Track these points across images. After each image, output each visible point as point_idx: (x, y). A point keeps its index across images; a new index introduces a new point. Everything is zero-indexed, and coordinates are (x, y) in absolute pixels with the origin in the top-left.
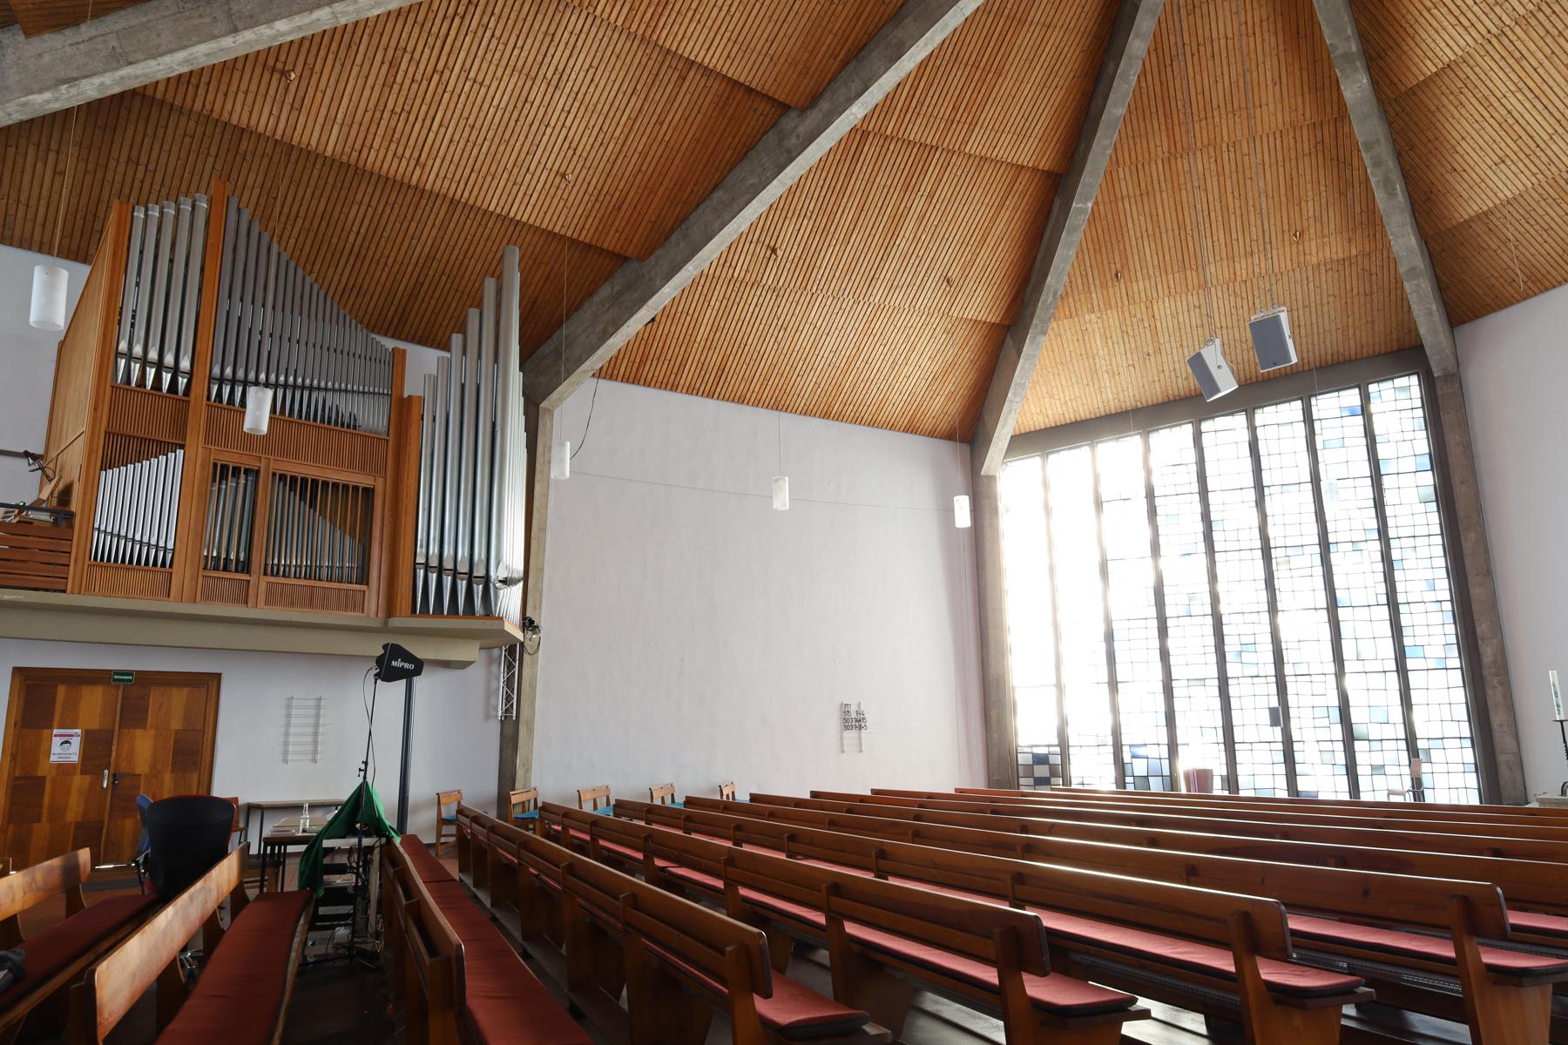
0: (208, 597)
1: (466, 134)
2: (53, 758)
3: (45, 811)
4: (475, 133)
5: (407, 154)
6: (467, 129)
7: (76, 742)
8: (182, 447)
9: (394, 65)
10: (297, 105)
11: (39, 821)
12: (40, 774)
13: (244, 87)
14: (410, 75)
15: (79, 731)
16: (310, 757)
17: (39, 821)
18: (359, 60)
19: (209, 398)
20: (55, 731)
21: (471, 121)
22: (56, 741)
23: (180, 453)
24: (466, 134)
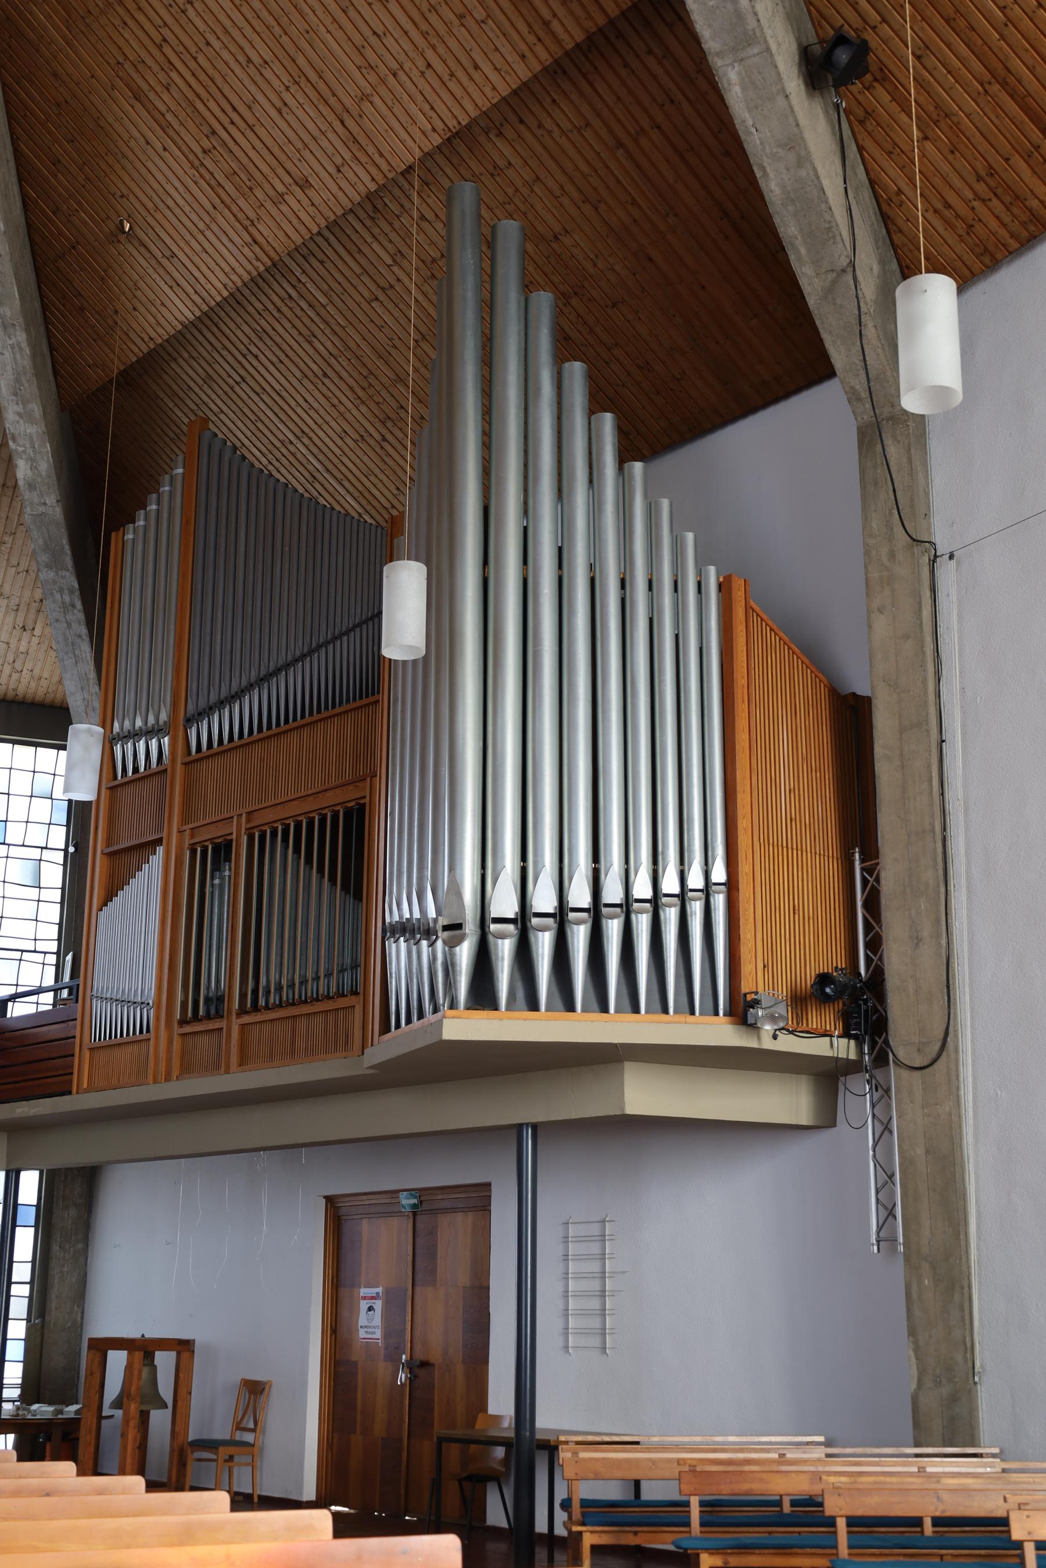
0: (187, 1068)
1: (276, 83)
2: (362, 1334)
3: (359, 1417)
4: (276, 66)
5: (280, 188)
6: (267, 73)
7: (378, 1305)
8: (159, 842)
9: (138, 96)
10: (168, 253)
11: (355, 1433)
12: (353, 1359)
13: (130, 283)
14: (159, 89)
15: (380, 1290)
16: (596, 1341)
17: (355, 1433)
18: (126, 136)
19: (189, 753)
20: (364, 1291)
21: (256, 59)
22: (364, 1305)
23: (160, 850)
24: (276, 83)
